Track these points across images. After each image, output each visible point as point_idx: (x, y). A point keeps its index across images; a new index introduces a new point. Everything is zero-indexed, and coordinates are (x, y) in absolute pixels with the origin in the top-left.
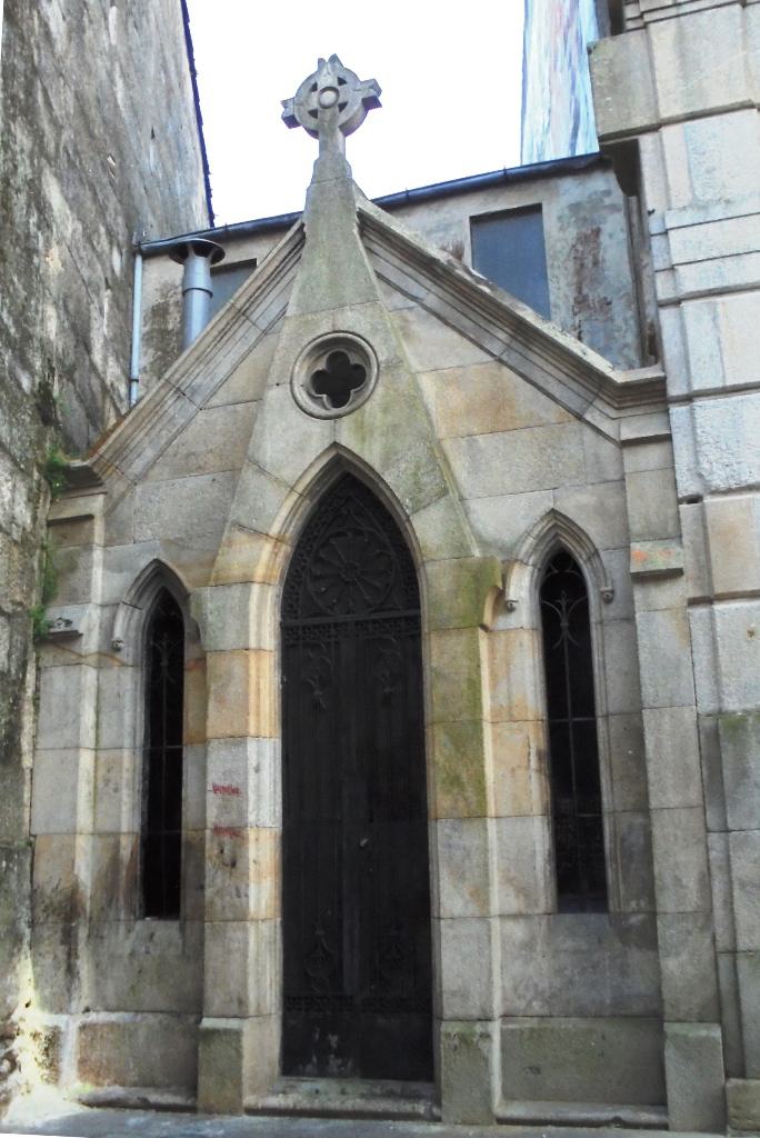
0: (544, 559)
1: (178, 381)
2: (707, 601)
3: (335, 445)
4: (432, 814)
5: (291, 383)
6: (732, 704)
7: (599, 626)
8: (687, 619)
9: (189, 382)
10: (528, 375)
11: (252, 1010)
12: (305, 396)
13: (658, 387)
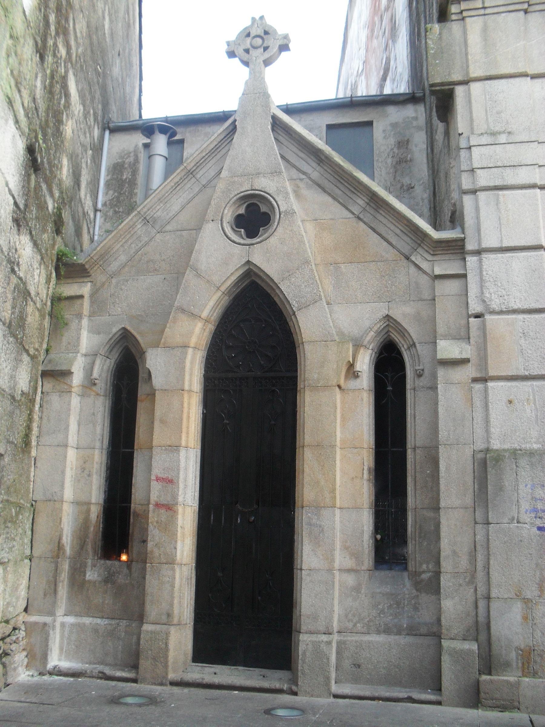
0: (380, 346)
1: (145, 213)
2: (484, 380)
3: (248, 262)
4: (298, 503)
5: (221, 220)
6: (496, 445)
7: (412, 391)
8: (471, 389)
9: (152, 214)
10: (376, 228)
11: (175, 621)
12: (229, 228)
13: (460, 243)
